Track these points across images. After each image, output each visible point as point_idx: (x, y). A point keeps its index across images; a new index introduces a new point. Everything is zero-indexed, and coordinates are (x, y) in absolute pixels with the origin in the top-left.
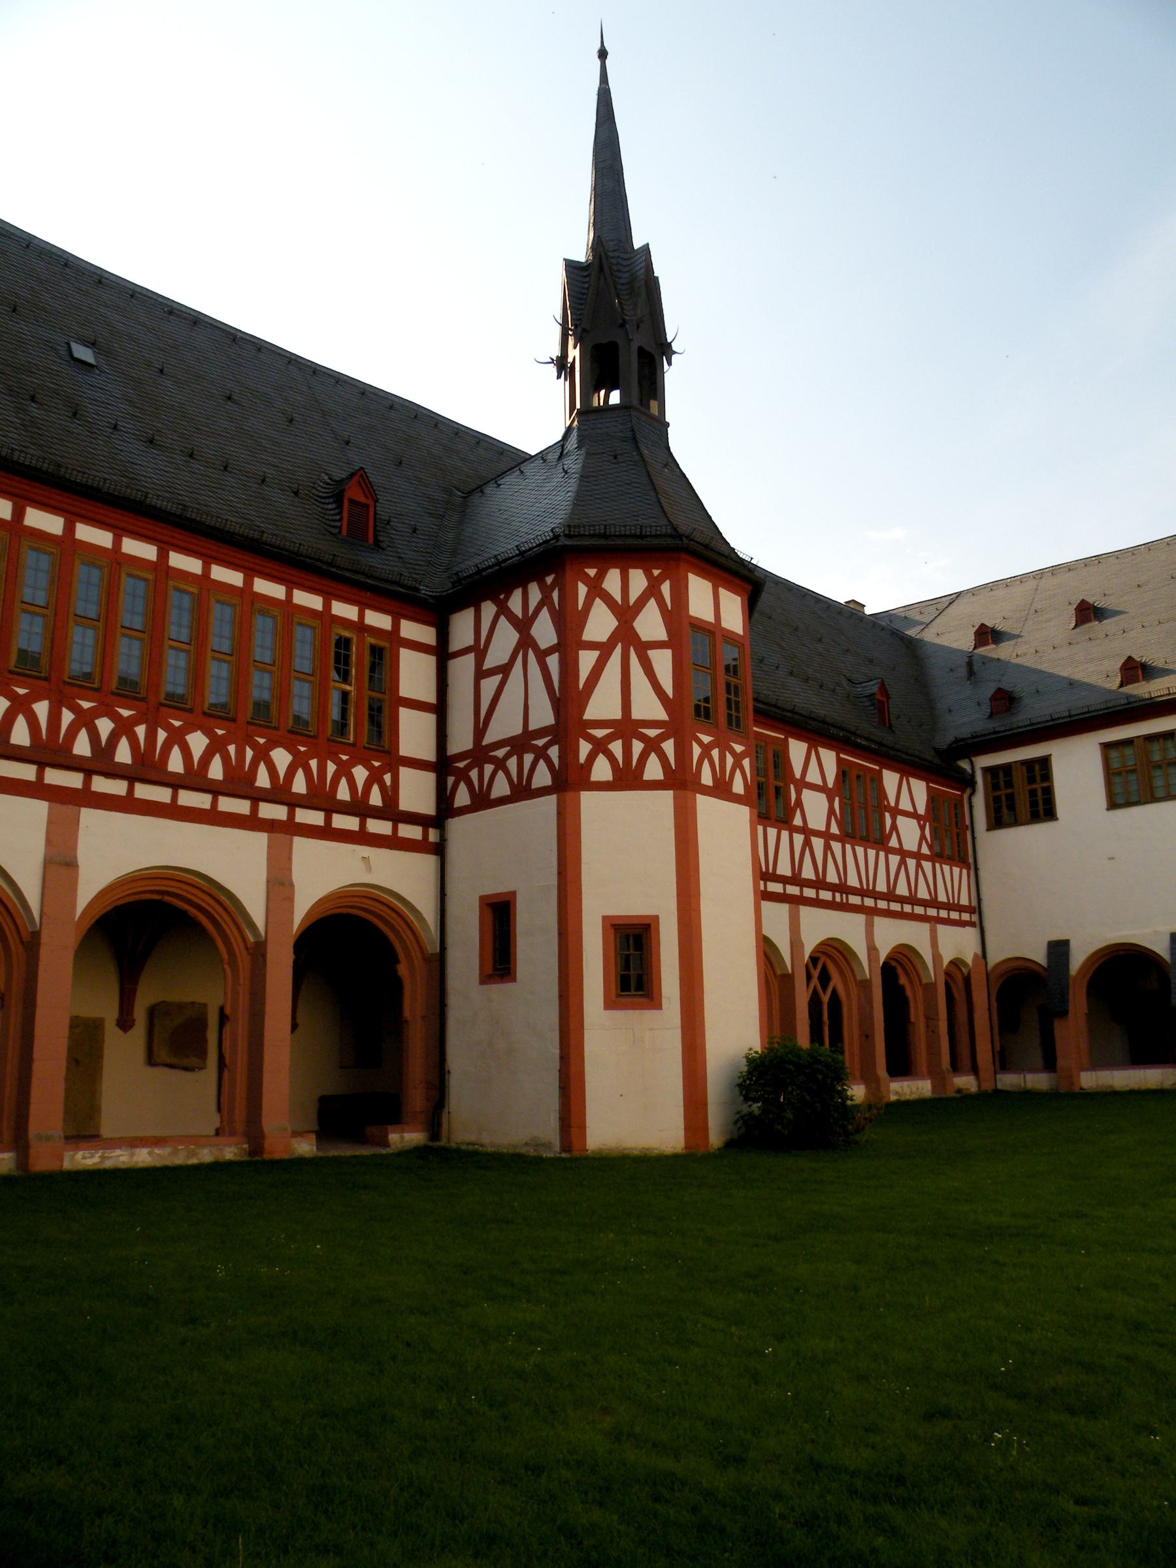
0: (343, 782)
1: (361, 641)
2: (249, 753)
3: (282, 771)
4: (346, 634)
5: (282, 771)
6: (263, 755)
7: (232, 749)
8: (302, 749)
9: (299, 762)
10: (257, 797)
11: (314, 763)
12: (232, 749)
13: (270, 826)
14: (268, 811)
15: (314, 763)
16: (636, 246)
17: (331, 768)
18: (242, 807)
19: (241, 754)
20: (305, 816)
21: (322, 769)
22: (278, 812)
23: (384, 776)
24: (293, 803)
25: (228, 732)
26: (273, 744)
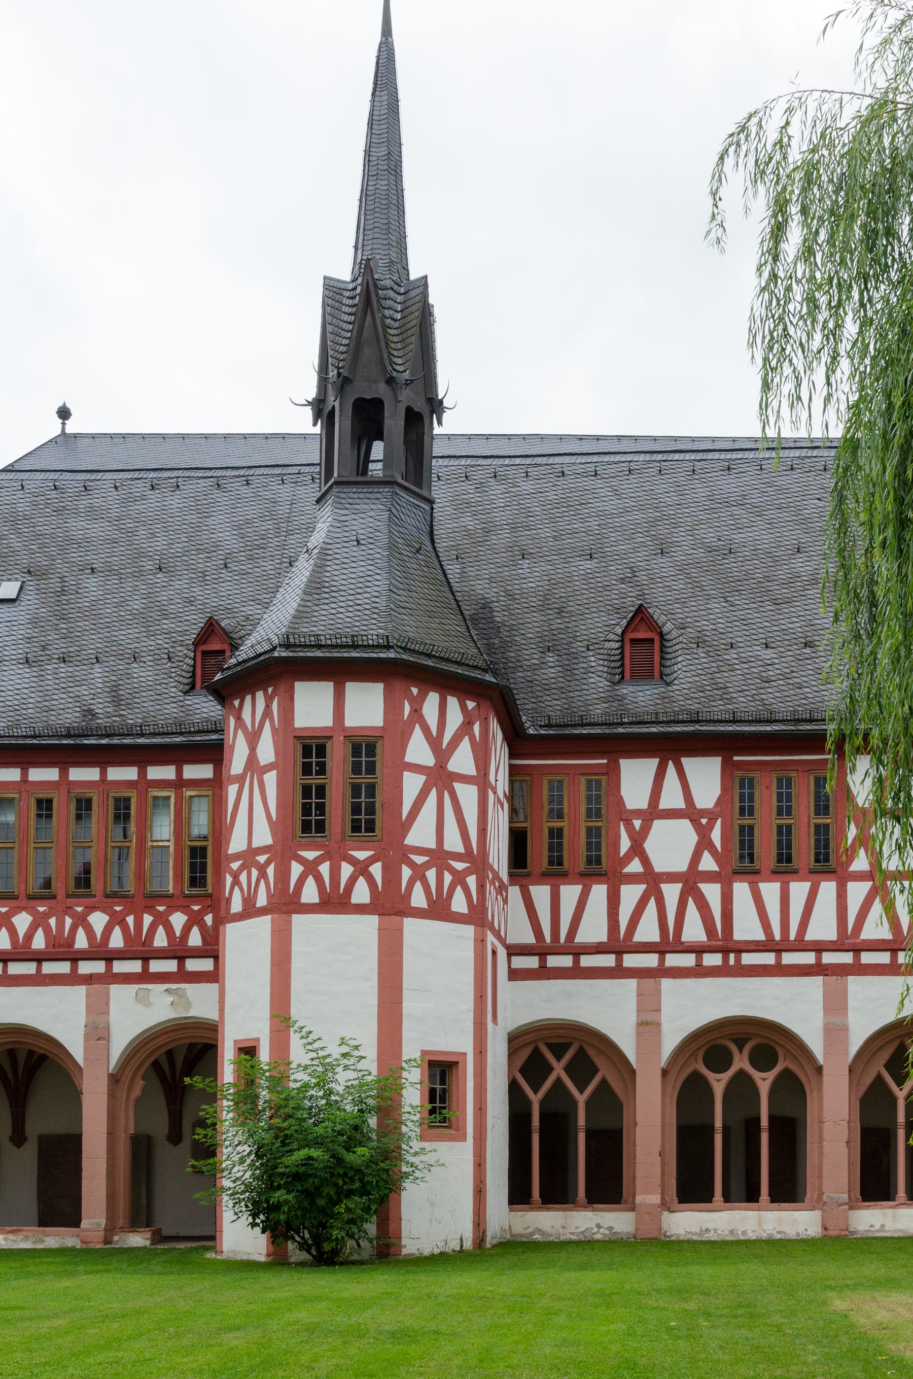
0: (161, 930)
1: (179, 798)
2: (68, 921)
3: (98, 930)
4: (164, 794)
5: (98, 930)
6: (81, 921)
7: (53, 921)
8: (118, 909)
9: (117, 920)
10: (75, 958)
11: (130, 920)
12: (53, 921)
13: (89, 979)
14: (86, 968)
15: (130, 920)
16: (412, 277)
17: (148, 919)
18: (64, 968)
19: (60, 924)
20: (120, 967)
21: (139, 923)
22: (99, 967)
23: (205, 918)
24: (110, 957)
25: (50, 908)
26: (91, 909)
